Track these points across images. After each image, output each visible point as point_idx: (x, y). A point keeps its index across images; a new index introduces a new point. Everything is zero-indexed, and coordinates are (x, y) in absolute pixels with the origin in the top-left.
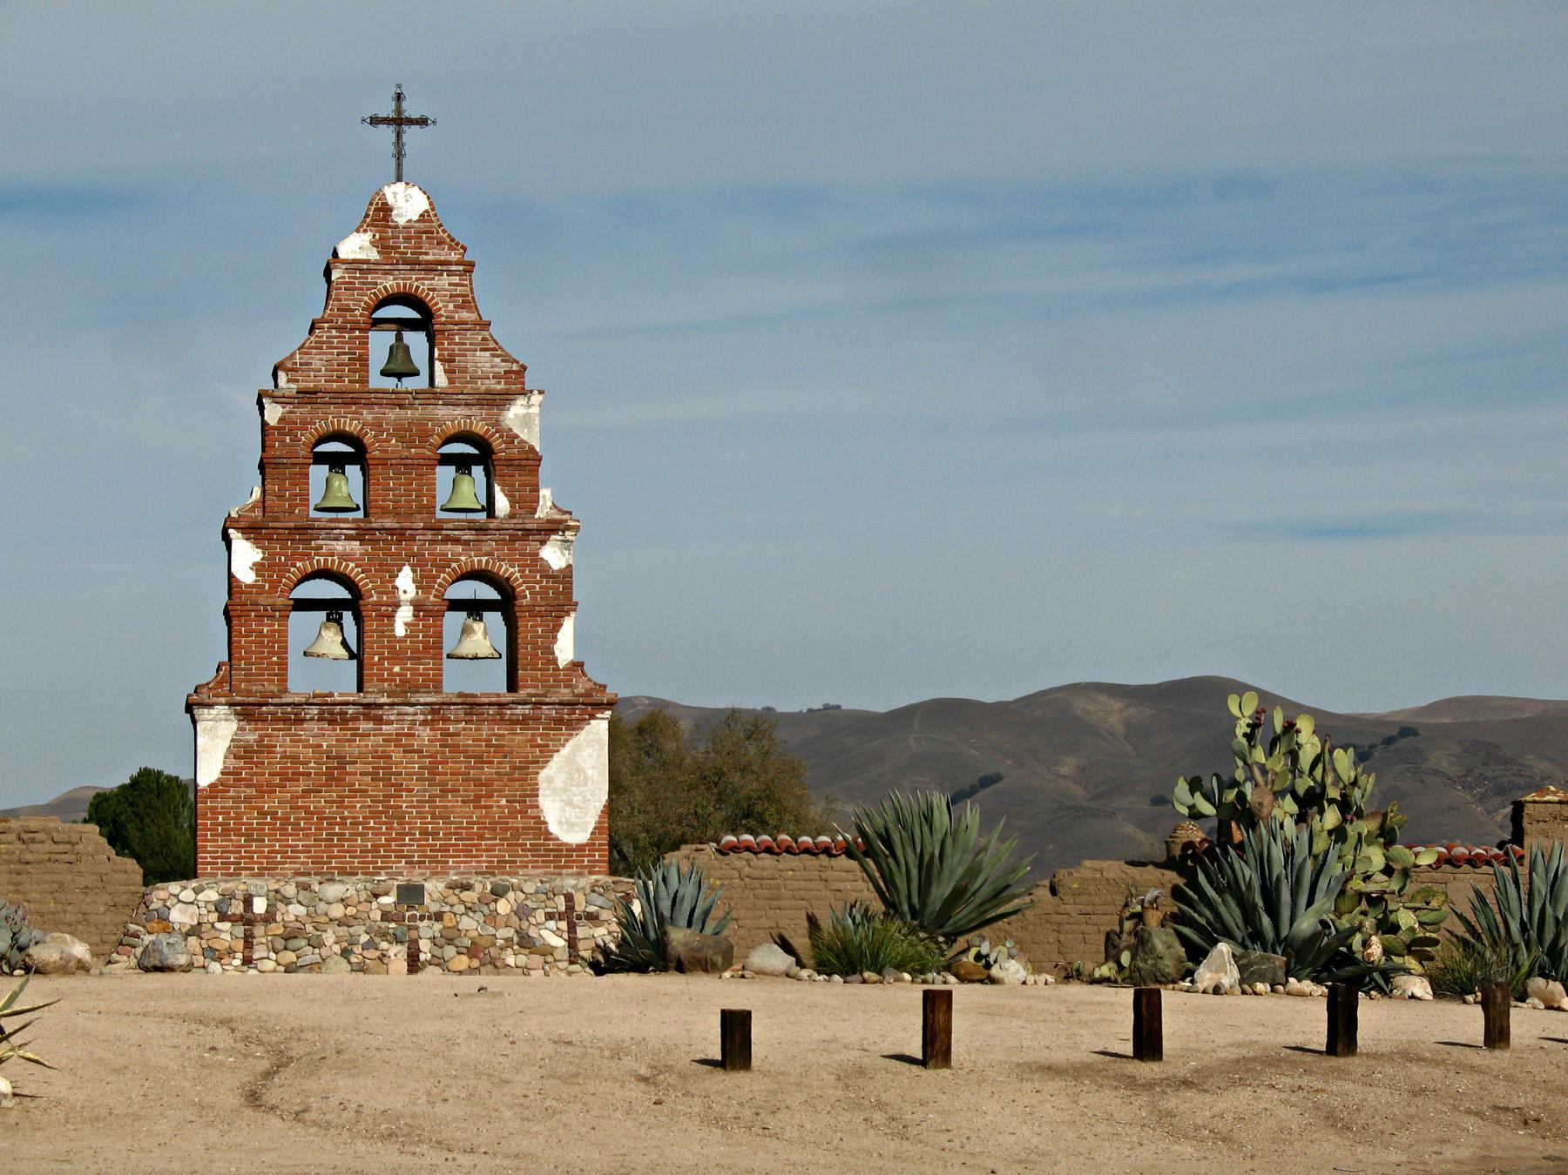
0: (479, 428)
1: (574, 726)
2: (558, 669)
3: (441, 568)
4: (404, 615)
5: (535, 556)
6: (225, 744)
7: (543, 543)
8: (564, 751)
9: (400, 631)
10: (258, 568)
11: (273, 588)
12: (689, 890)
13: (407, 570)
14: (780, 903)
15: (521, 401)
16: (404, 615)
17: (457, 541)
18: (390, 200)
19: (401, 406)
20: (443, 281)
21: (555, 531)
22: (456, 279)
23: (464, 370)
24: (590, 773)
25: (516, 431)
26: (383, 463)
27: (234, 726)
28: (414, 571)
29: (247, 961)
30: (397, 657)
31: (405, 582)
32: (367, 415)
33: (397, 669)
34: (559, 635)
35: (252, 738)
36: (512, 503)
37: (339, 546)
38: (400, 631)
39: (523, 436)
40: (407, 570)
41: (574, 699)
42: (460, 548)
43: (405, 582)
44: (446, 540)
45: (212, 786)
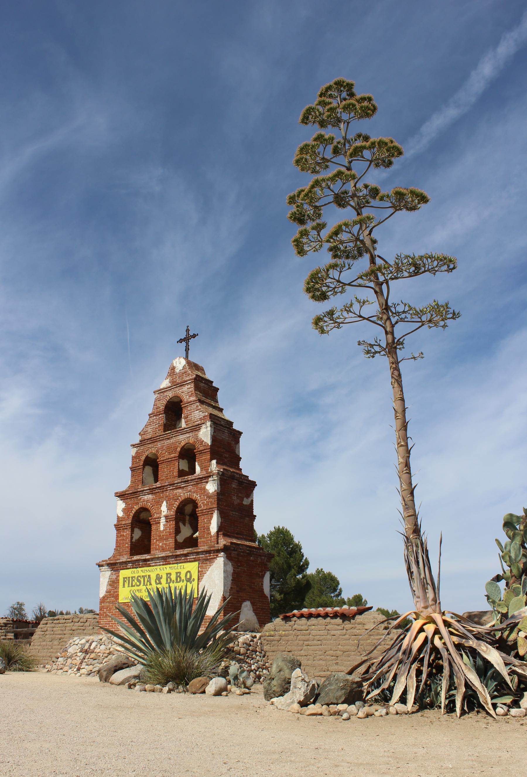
0: (191, 441)
1: (211, 561)
2: (211, 537)
3: (176, 500)
4: (163, 521)
5: (205, 488)
6: (107, 580)
7: (207, 482)
8: (208, 573)
9: (162, 528)
10: (124, 510)
11: (128, 518)
12: (277, 638)
13: (165, 503)
14: (310, 643)
15: (204, 426)
16: (163, 521)
17: (180, 488)
18: (175, 365)
19: (168, 439)
20: (185, 388)
21: (210, 476)
22: (189, 386)
23: (191, 420)
24: (217, 582)
25: (203, 439)
26: (163, 462)
27: (109, 573)
28: (167, 503)
29: (79, 669)
30: (161, 539)
31: (164, 508)
32: (159, 445)
33: (161, 544)
34: (212, 521)
35: (114, 577)
36: (201, 470)
37: (146, 497)
38: (162, 528)
39: (205, 440)
40: (165, 503)
41: (208, 549)
42: (180, 491)
43: (164, 508)
44: (177, 488)
45: (104, 597)
